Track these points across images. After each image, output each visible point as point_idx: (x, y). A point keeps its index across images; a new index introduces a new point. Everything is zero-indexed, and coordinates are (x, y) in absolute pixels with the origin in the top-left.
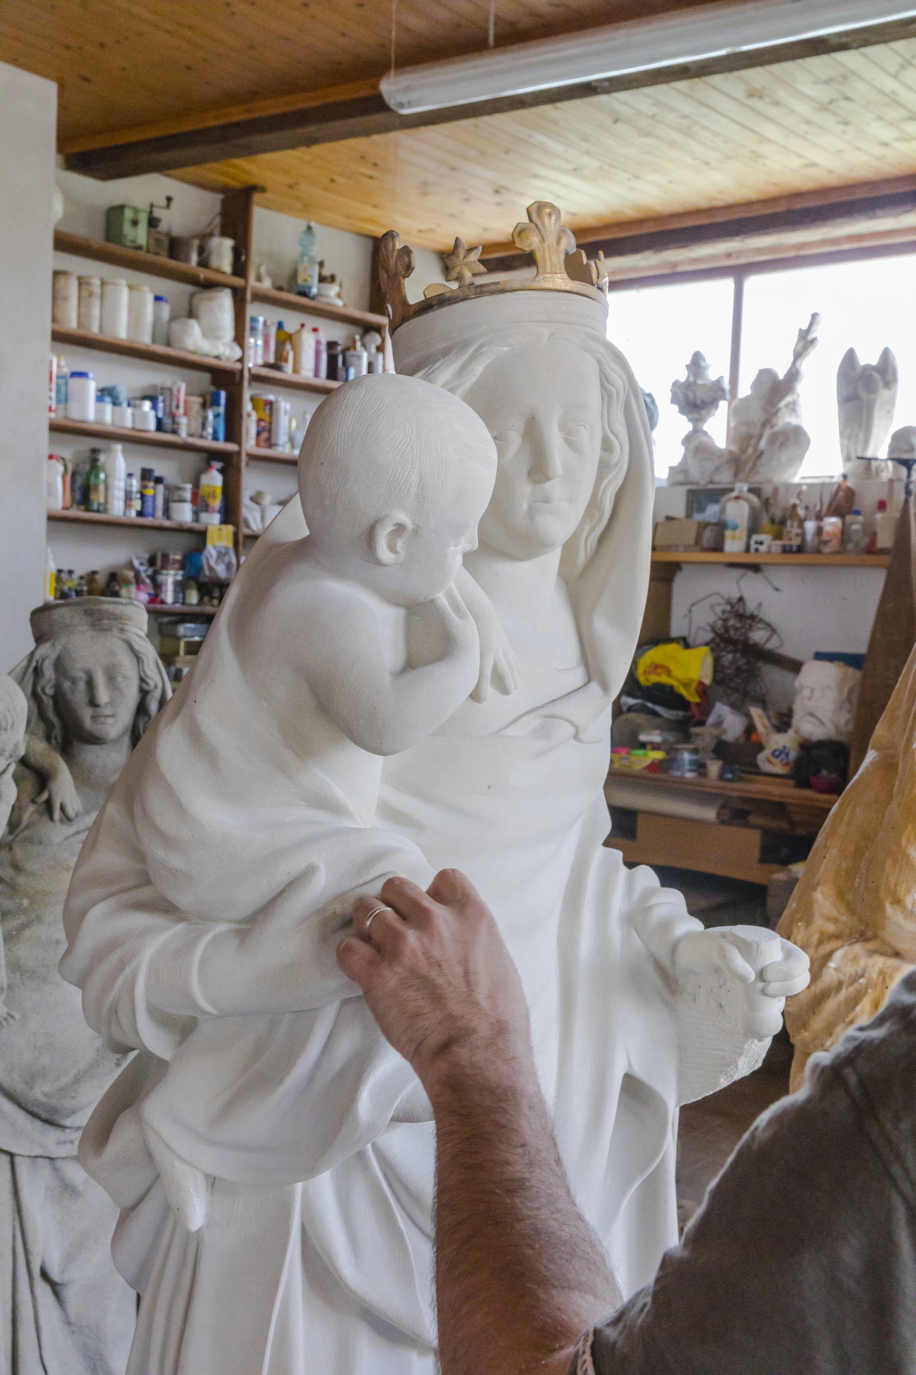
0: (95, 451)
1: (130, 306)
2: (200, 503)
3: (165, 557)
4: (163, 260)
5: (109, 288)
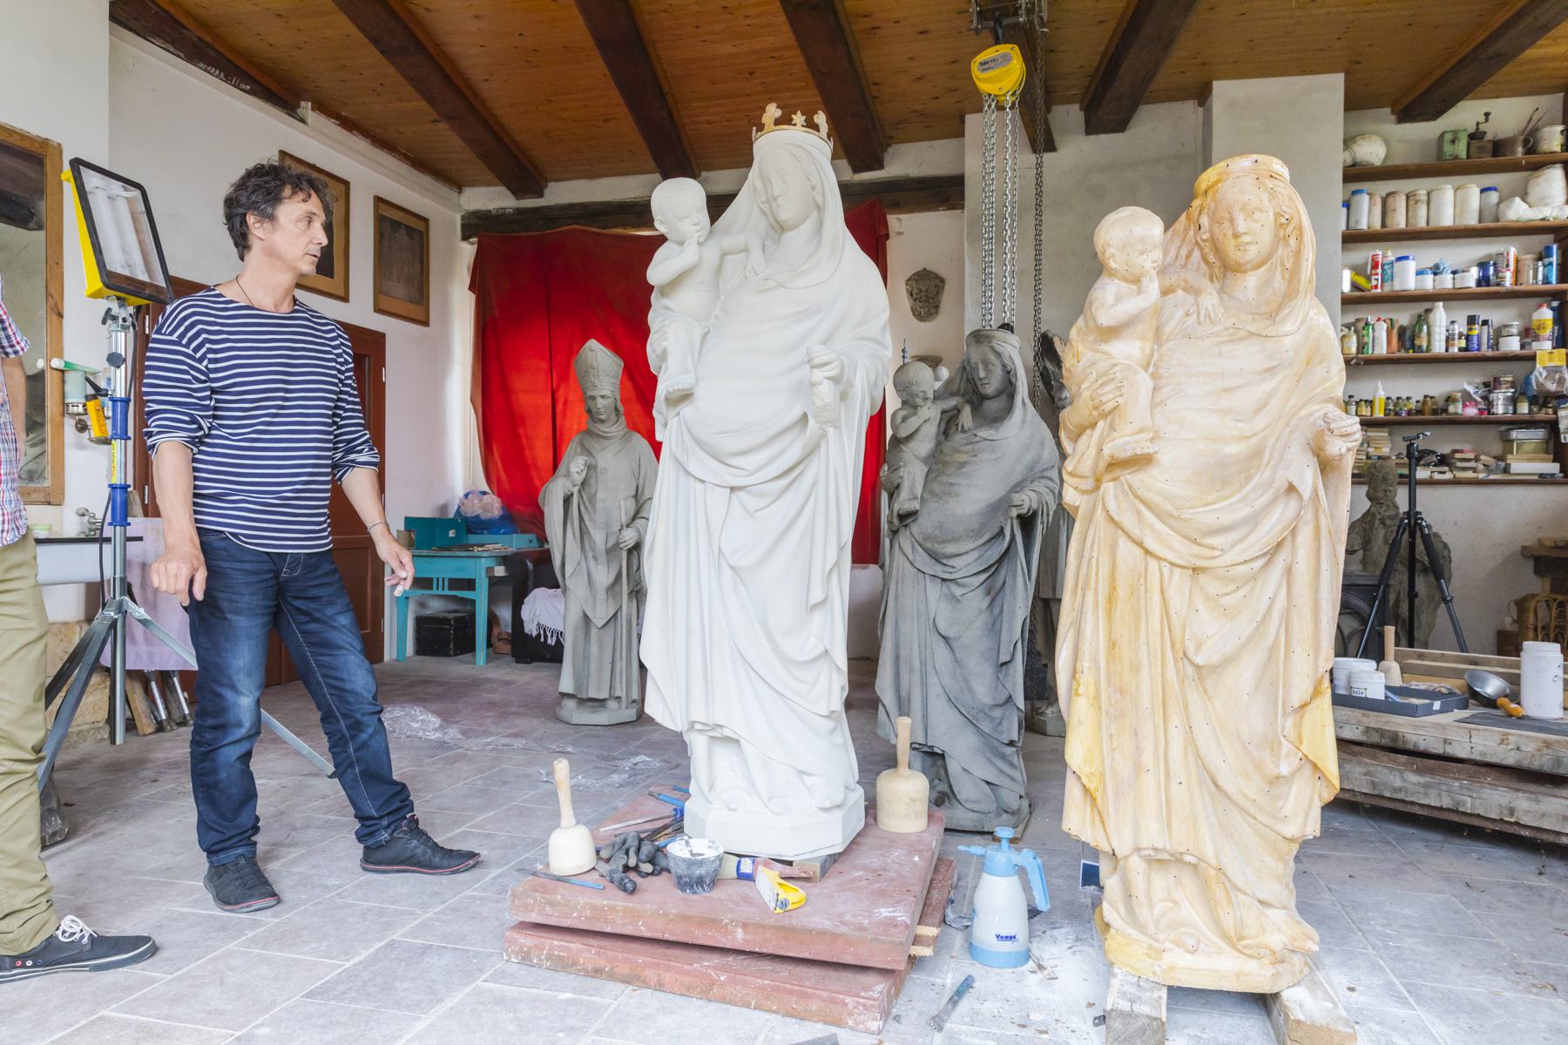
0: (1428, 311)
1: (1455, 201)
2: (1528, 334)
3: (1496, 380)
4: (1488, 159)
5: (1433, 195)
